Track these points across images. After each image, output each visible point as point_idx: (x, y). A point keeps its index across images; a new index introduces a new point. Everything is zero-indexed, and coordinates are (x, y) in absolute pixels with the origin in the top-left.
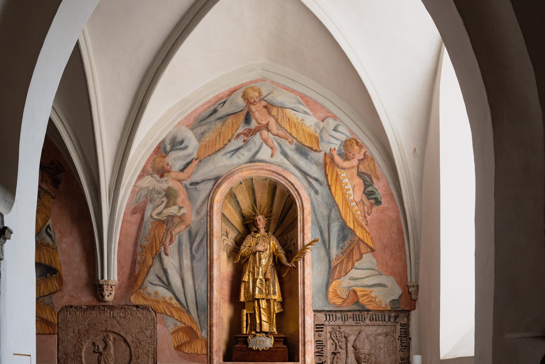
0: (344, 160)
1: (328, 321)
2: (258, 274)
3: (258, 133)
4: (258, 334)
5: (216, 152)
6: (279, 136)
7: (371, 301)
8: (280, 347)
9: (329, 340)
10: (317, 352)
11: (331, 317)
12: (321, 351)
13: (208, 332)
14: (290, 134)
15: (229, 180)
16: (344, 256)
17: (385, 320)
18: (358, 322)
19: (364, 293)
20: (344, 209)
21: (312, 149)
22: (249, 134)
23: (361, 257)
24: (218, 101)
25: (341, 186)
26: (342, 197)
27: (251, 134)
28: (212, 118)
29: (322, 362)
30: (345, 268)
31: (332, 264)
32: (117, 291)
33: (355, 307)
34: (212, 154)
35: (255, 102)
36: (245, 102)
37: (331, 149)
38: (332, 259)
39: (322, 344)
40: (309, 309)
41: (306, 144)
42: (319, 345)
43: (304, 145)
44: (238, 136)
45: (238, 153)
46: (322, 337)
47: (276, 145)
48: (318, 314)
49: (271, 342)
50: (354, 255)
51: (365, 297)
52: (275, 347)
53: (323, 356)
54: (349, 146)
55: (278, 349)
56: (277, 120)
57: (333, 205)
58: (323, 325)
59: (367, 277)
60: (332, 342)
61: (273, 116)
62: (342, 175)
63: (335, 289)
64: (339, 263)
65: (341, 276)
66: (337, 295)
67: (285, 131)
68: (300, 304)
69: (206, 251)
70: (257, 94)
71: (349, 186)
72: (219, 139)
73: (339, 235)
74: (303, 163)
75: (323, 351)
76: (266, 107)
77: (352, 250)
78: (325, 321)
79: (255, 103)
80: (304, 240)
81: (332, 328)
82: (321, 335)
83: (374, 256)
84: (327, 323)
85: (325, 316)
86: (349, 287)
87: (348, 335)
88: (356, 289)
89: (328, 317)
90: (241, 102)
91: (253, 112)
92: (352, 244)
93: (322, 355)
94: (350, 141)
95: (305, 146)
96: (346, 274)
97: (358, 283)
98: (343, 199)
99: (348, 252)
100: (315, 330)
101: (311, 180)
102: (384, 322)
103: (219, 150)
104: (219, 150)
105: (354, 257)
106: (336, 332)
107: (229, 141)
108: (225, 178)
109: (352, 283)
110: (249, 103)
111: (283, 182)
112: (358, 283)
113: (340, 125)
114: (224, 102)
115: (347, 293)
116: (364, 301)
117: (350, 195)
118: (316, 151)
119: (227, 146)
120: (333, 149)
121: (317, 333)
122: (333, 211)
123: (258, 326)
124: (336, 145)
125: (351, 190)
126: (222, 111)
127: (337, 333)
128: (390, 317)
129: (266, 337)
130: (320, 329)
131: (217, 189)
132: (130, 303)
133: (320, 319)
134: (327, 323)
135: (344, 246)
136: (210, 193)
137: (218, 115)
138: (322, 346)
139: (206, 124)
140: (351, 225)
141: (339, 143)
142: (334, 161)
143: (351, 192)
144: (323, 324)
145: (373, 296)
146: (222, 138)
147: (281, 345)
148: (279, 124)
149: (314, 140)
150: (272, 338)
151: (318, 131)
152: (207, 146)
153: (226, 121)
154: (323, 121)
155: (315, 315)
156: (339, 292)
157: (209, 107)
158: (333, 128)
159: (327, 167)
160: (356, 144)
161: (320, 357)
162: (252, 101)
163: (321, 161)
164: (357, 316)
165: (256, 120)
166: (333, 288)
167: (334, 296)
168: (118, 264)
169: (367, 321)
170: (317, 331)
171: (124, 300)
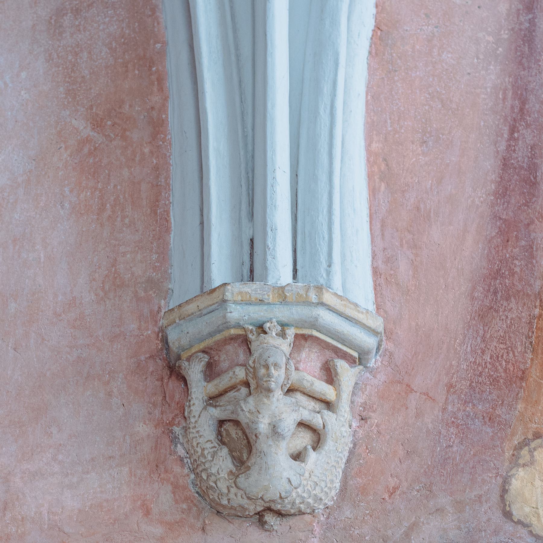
32: (375, 418)
132: (509, 527)
168: (373, 192)
171: (443, 500)
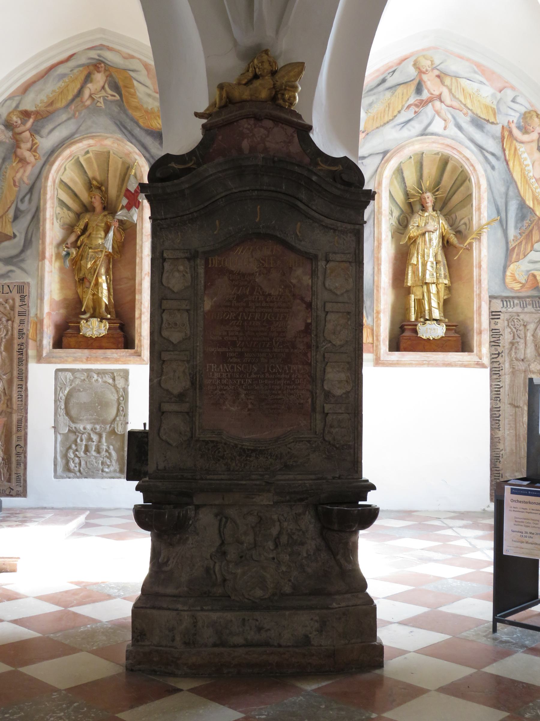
0: (524, 134)
2: (428, 256)
3: (430, 104)
4: (428, 322)
5: (385, 124)
6: (452, 107)
10: (494, 342)
11: (508, 303)
12: (498, 340)
13: (375, 318)
14: (465, 105)
15: (398, 155)
16: (523, 237)
20: (522, 186)
21: (488, 121)
22: (421, 105)
24: (387, 70)
25: (520, 161)
26: (520, 173)
27: (424, 104)
28: (381, 88)
31: (510, 245)
34: (380, 127)
35: (427, 71)
36: (416, 71)
37: (509, 122)
39: (499, 332)
41: (482, 116)
43: (479, 117)
44: (409, 107)
45: (408, 126)
46: (499, 325)
47: (450, 117)
48: (494, 301)
53: (499, 346)
54: (529, 118)
56: (450, 90)
57: (510, 182)
58: (500, 312)
60: (509, 330)
61: (447, 86)
62: (521, 150)
63: (513, 272)
66: (515, 280)
67: (459, 103)
68: (475, 289)
69: (373, 231)
70: (429, 63)
71: (528, 162)
72: (388, 110)
73: (517, 214)
74: (478, 136)
75: (499, 340)
76: (438, 76)
77: (531, 231)
78: (502, 308)
79: (427, 72)
80: (480, 219)
84: (504, 310)
86: (528, 271)
87: (527, 322)
88: (536, 273)
89: (505, 303)
90: (412, 72)
91: (425, 82)
92: (531, 224)
93: (498, 344)
94: (529, 113)
95: (481, 118)
96: (525, 256)
98: (521, 175)
99: (527, 232)
101: (487, 154)
103: (388, 122)
104: (388, 122)
107: (399, 112)
108: (395, 152)
109: (532, 266)
110: (421, 72)
111: (457, 156)
113: (518, 96)
114: (394, 71)
115: (526, 277)
117: (529, 171)
118: (493, 123)
119: (396, 118)
120: (511, 121)
122: (511, 189)
123: (427, 312)
124: (514, 117)
125: (531, 166)
126: (391, 82)
127: (515, 321)
131: (386, 165)
134: (504, 310)
135: (523, 226)
136: (378, 168)
137: (387, 85)
138: (499, 335)
139: (374, 94)
140: (530, 203)
141: (517, 115)
142: (512, 135)
143: (531, 167)
146: (391, 110)
147: (452, 334)
148: (453, 94)
149: (490, 111)
151: (495, 103)
152: (375, 118)
153: (395, 91)
154: (500, 91)
155: (490, 301)
156: (517, 277)
157: (377, 77)
158: (511, 99)
159: (505, 140)
160: (536, 117)
161: (496, 347)
162: (424, 70)
163: (499, 134)
164: (537, 302)
165: (428, 91)
167: (512, 280)
170: (492, 319)
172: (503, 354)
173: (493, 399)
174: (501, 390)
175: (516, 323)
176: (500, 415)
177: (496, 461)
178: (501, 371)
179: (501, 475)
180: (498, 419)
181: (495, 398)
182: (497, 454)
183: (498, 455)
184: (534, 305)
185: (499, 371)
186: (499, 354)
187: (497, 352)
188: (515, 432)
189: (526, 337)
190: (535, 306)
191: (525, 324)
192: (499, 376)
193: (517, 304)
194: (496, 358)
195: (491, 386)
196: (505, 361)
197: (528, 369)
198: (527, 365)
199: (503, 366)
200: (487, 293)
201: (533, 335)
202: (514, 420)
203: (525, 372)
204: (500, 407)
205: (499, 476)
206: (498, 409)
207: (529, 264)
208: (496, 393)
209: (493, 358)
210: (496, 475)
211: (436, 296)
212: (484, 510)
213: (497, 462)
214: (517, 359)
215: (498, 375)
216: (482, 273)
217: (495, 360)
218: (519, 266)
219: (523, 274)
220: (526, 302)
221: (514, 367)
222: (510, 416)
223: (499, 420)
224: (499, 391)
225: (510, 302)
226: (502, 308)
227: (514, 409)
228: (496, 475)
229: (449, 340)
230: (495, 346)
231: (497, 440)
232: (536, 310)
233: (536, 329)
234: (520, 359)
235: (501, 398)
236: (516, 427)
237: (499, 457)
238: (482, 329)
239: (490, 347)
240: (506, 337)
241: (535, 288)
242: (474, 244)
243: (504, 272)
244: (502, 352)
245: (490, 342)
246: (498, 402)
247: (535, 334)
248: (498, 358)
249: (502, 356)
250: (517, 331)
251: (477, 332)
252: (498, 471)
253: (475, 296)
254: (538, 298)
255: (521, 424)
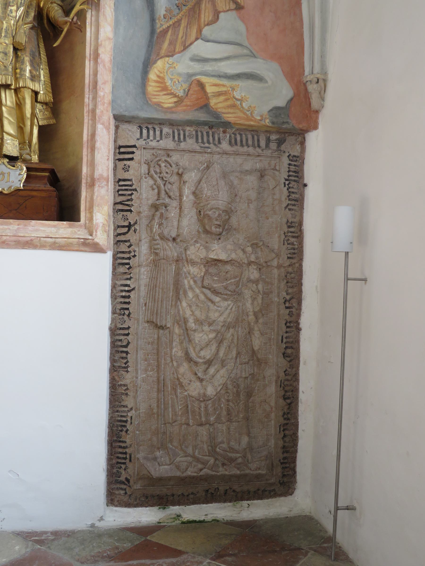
1: (145, 140)
7: (233, 106)
8: (40, 188)
9: (146, 178)
10: (121, 203)
11: (151, 132)
12: (128, 200)
16: (182, 13)
17: (259, 146)
18: (207, 145)
19: (220, 90)
23: (216, 18)
29: (130, 223)
30: (182, 37)
31: (158, 25)
33: (202, 116)
38: (157, 16)
40: (105, 112)
42: (124, 188)
46: (131, 171)
48: (124, 127)
49: (21, 176)
50: (203, 12)
51: (222, 98)
52: (28, 188)
53: (130, 211)
55: (34, 193)
58: (134, 146)
59: (227, 58)
60: (151, 182)
63: (161, 75)
64: (171, 25)
65: (174, 51)
66: (164, 88)
68: (86, 100)
75: (131, 200)
78: (138, 139)
81: (153, 155)
82: (129, 167)
83: (243, 19)
85: (139, 130)
86: (190, 75)
87: (184, 169)
88: (204, 79)
89: (145, 131)
93: (128, 208)
96: (185, 48)
97: (208, 67)
100: (117, 158)
102: (257, 149)
105: (202, 16)
106: (160, 162)
109: (197, 67)
112: (208, 67)
115: (185, 86)
116: (220, 105)
121: (121, 165)
127: (163, 165)
128: (268, 140)
129: (9, 166)
130: (127, 156)
133: (128, 134)
134: (141, 143)
144: (133, 144)
145: (237, 97)
150: (22, 169)
155: (117, 127)
156: (169, 83)
161: (125, 213)
164: (205, 134)
166: (158, 73)
169: (225, 146)
170: (120, 160)
172: (137, 227)
173: (118, 311)
174: (132, 294)
175: (163, 168)
176: (129, 343)
177: (120, 429)
178: (133, 259)
179: (128, 457)
180: (124, 349)
181: (120, 310)
182: (122, 416)
183: (124, 419)
184: (200, 138)
185: (129, 258)
186: (129, 226)
187: (126, 224)
188: (156, 375)
189: (181, 196)
190: (200, 141)
191: (180, 172)
192: (128, 269)
193: (168, 134)
194: (124, 234)
195: (114, 287)
196: (140, 240)
197: (184, 256)
198: (182, 250)
199: (137, 249)
200: (110, 109)
201: (194, 193)
202: (155, 351)
203: (177, 261)
204: (129, 328)
205: (125, 459)
206: (126, 332)
207: (192, 63)
208: (123, 300)
209: (120, 234)
210: (120, 455)
211: (14, 112)
212: (93, 526)
213: (121, 431)
214: (163, 238)
215: (128, 266)
216: (100, 68)
217: (122, 238)
218: (175, 65)
219: (180, 80)
220: (184, 131)
221: (157, 251)
222: (149, 343)
223: (127, 353)
224: (129, 297)
225: (154, 129)
226: (138, 139)
227: (156, 331)
228: (120, 455)
229: (33, 197)
230: (122, 210)
231: (122, 390)
232: (201, 147)
233: (200, 181)
234: (169, 237)
235: (131, 310)
236: (158, 366)
237: (126, 421)
238: (96, 175)
239: (114, 213)
240: (144, 196)
241: (201, 108)
242: (88, 16)
243: (145, 72)
244: (136, 223)
245: (115, 204)
246: (125, 317)
247: (197, 192)
248: (127, 235)
249: (135, 231)
250: (164, 185)
251: (87, 183)
252: (124, 448)
253: (85, 114)
254: (207, 127)
255: (169, 360)
